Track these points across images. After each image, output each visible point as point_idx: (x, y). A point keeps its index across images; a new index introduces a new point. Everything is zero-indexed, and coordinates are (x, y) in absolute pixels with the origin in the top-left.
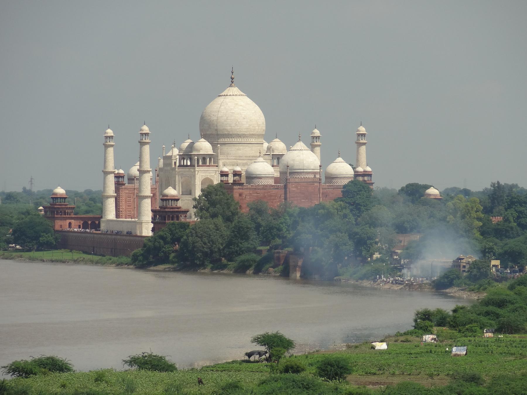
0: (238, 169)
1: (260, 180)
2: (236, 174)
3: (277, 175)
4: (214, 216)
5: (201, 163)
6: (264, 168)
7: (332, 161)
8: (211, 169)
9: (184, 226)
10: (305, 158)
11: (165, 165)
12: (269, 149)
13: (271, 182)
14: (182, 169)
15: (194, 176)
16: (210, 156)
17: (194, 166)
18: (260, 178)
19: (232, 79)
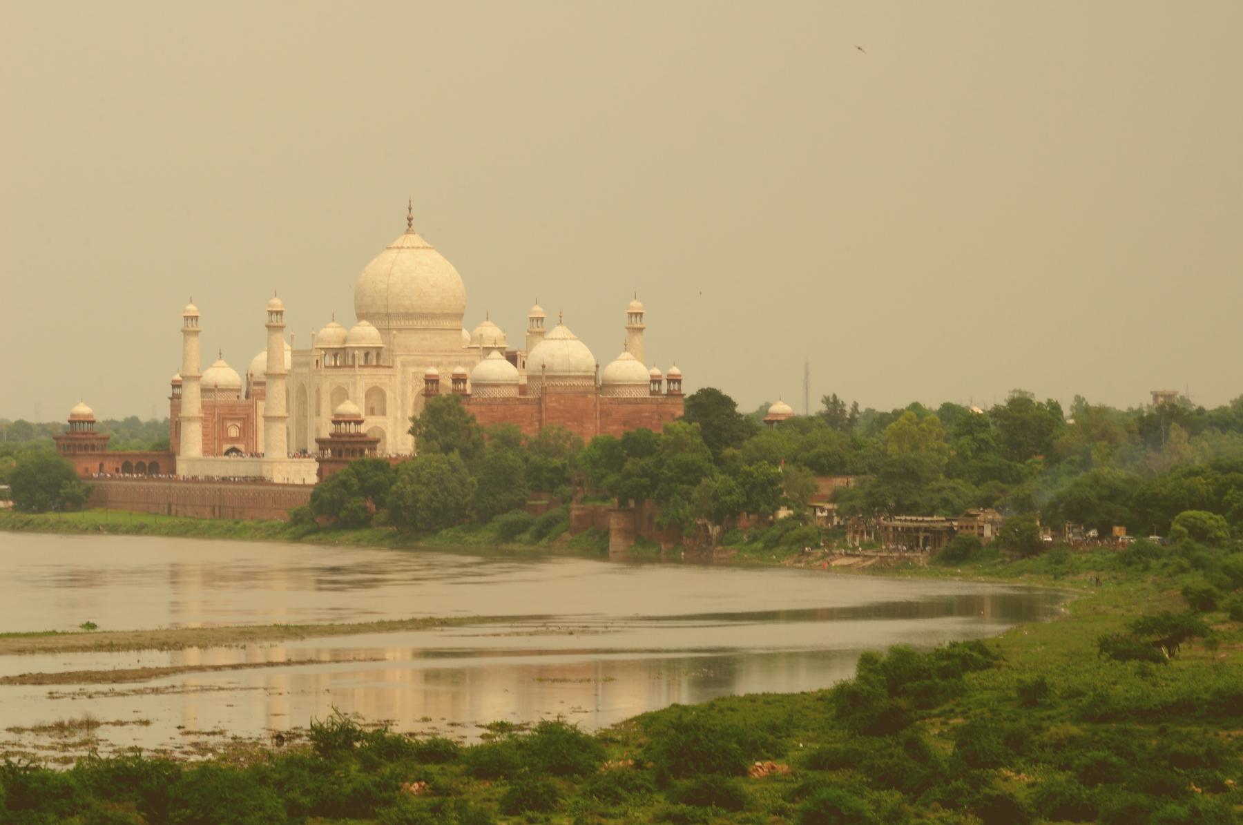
0: (460, 370)
1: (497, 390)
2: (458, 379)
3: (524, 381)
4: (447, 449)
5: (362, 363)
6: (496, 368)
7: (614, 357)
8: (381, 371)
9: (381, 465)
10: (564, 350)
11: (294, 364)
12: (473, 339)
13: (514, 393)
14: (329, 372)
15: (354, 384)
16: (378, 350)
17: (353, 366)
18: (497, 386)
19: (410, 219)
